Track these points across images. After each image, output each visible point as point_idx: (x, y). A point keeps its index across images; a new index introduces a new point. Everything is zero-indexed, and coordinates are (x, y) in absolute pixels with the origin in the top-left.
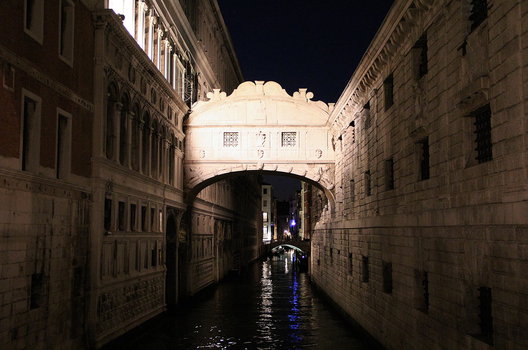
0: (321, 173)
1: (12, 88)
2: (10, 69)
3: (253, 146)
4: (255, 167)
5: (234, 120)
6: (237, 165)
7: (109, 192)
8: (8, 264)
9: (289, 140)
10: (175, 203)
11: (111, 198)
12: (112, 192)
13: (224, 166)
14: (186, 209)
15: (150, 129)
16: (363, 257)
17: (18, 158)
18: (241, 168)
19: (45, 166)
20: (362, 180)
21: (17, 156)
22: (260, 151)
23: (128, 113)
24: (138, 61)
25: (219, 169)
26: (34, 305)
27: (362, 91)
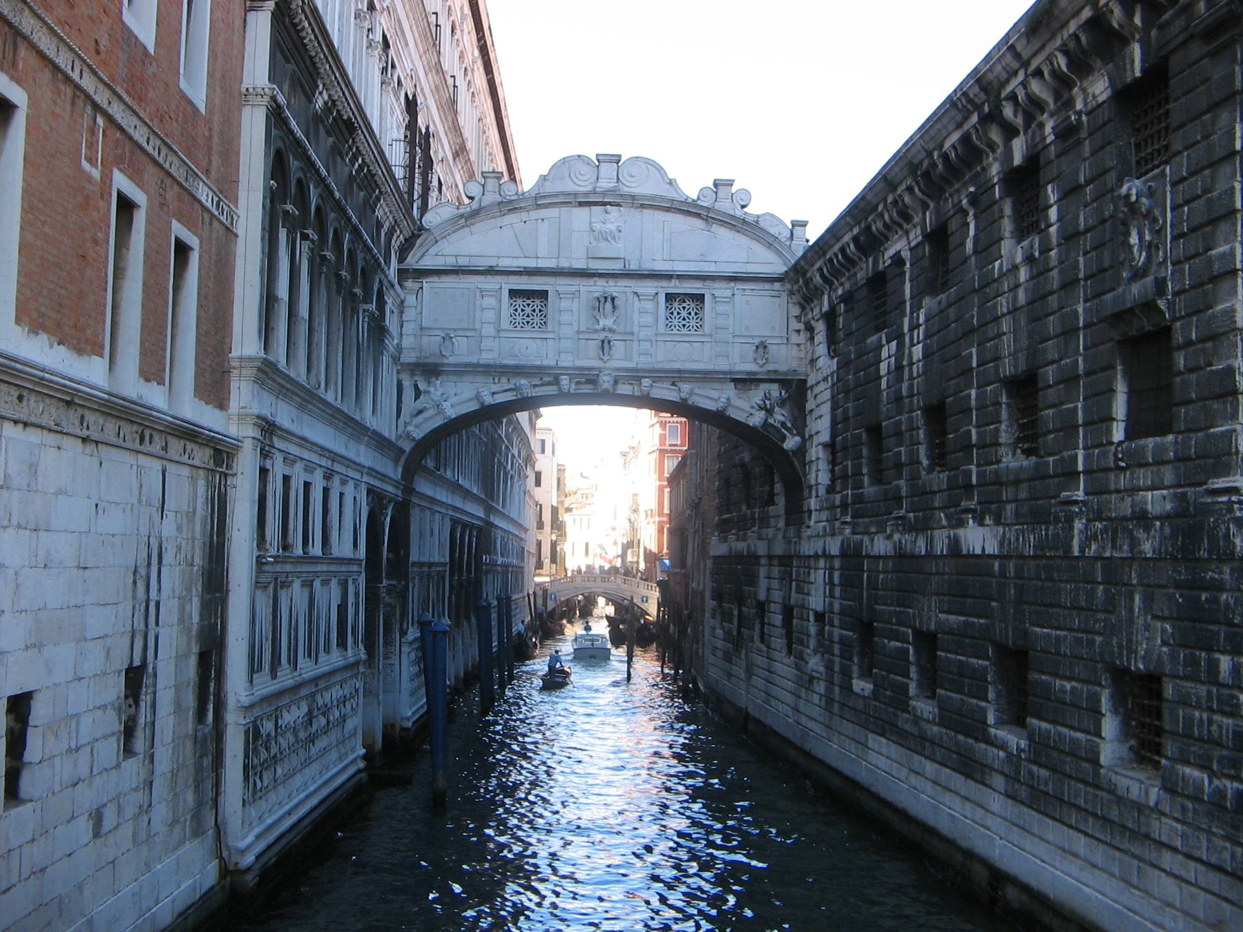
0: (769, 407)
1: (97, 168)
2: (95, 120)
7: (267, 448)
8: (85, 640)
9: (684, 314)
10: (383, 477)
11: (268, 466)
12: (273, 451)
14: (400, 493)
15: (338, 277)
16: (918, 634)
17: (102, 356)
18: (555, 388)
19: (147, 380)
20: (912, 429)
21: (97, 350)
22: (606, 342)
23: (302, 234)
24: (326, 97)
25: (495, 388)
26: (128, 751)
27: (923, 194)
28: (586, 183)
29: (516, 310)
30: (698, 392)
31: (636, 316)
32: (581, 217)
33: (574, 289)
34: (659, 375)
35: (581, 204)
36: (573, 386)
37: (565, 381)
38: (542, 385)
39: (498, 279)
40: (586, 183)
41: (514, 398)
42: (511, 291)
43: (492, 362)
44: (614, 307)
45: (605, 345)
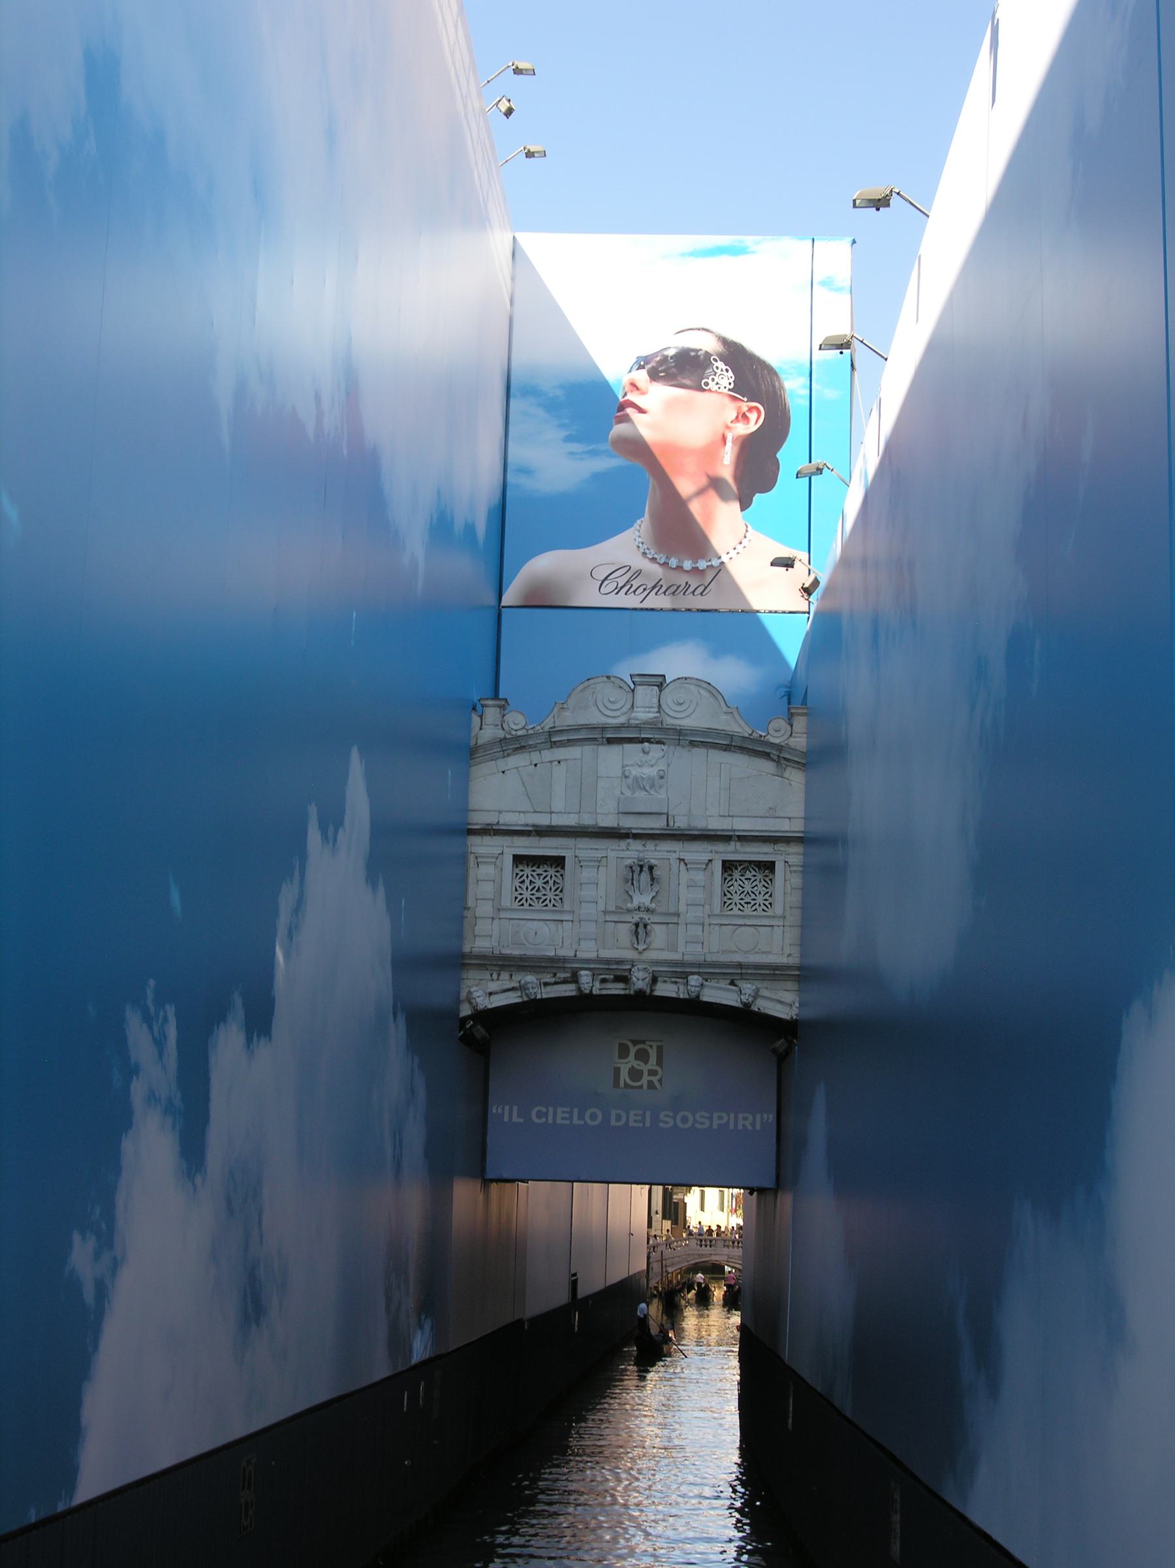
3: (616, 907)
4: (621, 985)
5: (552, 812)
6: (558, 975)
9: (748, 887)
13: (511, 976)
18: (573, 987)
22: (641, 926)
25: (493, 986)
28: (618, 713)
29: (523, 882)
30: (764, 992)
31: (683, 890)
32: (611, 759)
33: (599, 854)
34: (710, 970)
35: (610, 741)
36: (597, 985)
37: (585, 977)
38: (556, 983)
39: (498, 840)
40: (618, 713)
41: (519, 1000)
42: (514, 856)
43: (488, 952)
44: (653, 879)
45: (640, 929)
